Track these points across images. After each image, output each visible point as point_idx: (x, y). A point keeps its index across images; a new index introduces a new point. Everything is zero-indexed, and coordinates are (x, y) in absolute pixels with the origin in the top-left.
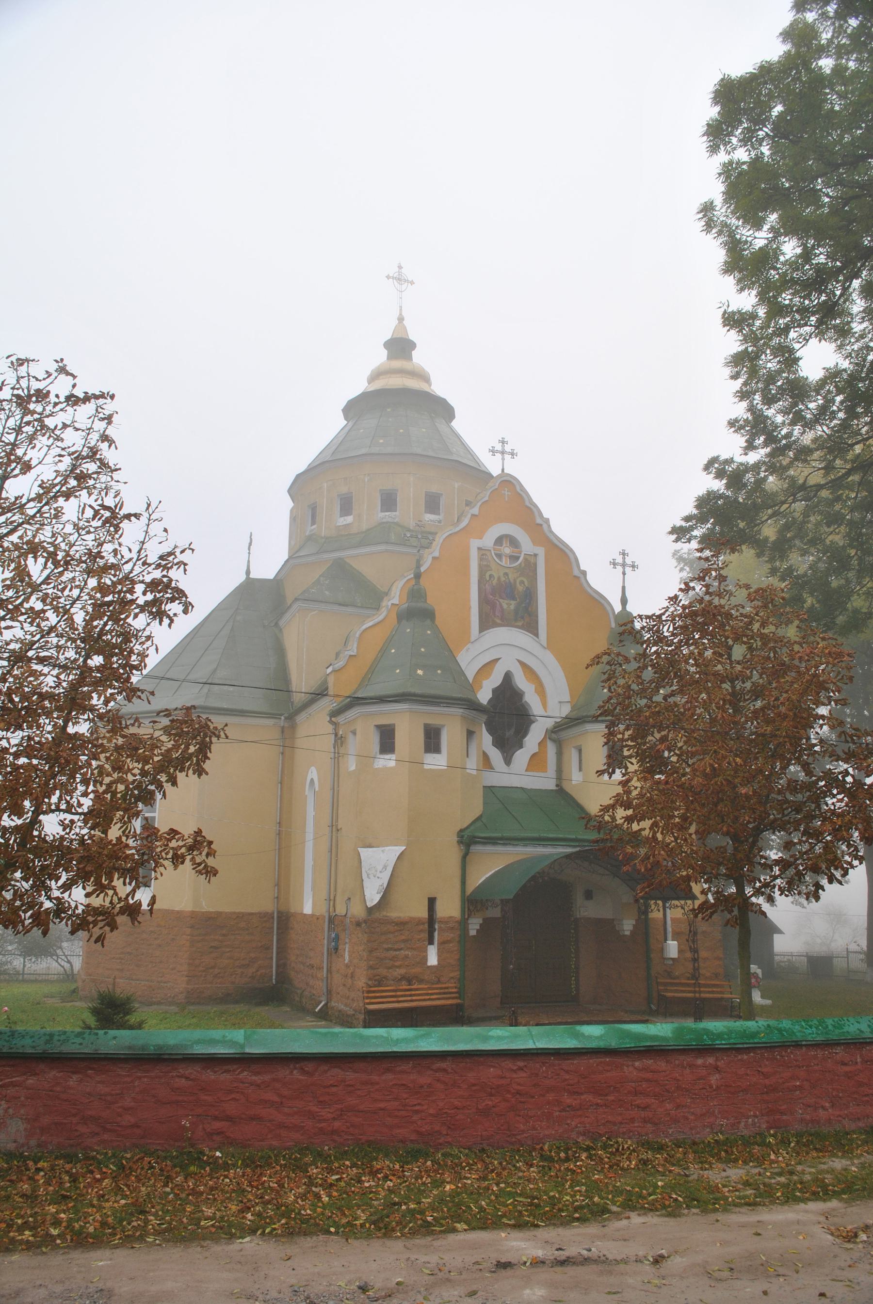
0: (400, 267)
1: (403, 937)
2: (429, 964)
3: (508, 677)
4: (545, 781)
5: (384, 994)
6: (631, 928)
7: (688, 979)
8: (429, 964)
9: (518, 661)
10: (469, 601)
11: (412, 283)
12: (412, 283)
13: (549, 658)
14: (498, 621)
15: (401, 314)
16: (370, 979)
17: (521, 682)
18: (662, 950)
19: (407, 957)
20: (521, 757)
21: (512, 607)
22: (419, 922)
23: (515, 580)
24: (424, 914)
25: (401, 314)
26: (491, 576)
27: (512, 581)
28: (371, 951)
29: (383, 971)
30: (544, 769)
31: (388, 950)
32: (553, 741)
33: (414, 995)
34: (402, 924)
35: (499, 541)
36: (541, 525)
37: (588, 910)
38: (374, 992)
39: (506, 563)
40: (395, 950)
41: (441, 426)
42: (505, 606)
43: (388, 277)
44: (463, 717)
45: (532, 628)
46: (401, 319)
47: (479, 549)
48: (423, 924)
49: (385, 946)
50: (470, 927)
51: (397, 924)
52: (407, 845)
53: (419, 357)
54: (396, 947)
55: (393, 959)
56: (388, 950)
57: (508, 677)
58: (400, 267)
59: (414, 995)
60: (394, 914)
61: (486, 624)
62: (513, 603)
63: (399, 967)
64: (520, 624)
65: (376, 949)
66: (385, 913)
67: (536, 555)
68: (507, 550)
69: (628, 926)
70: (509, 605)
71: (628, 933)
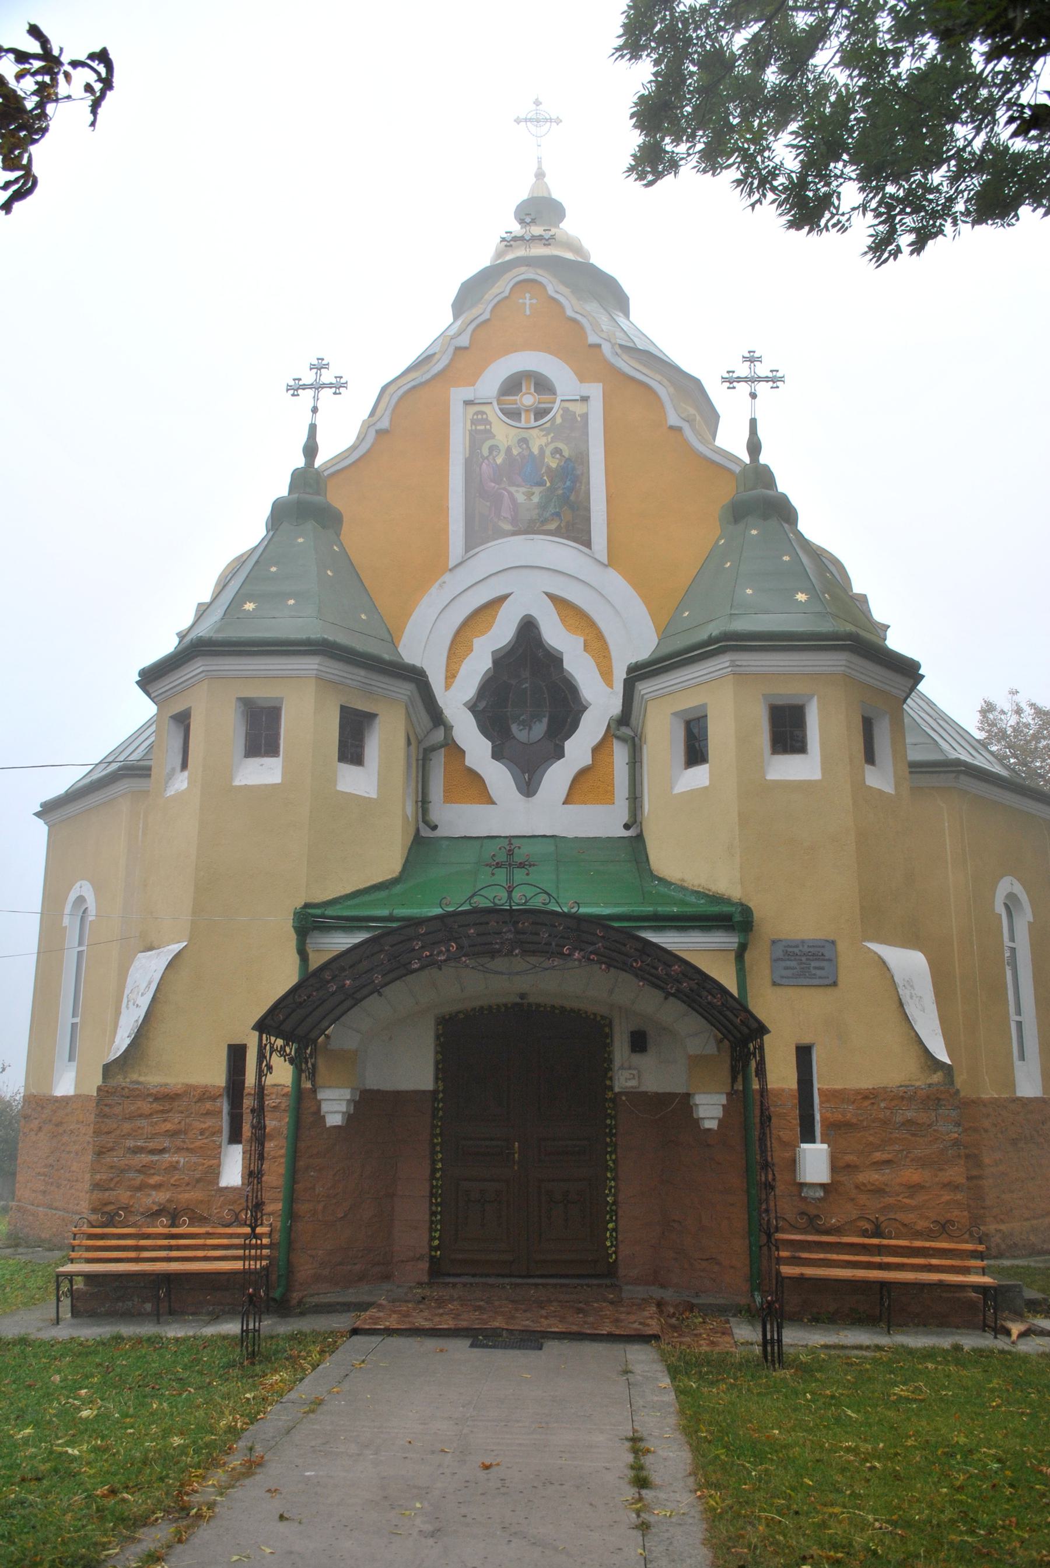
0: (537, 103)
1: (169, 1126)
2: (223, 1183)
3: (528, 628)
4: (604, 821)
5: (225, 1241)
6: (719, 1112)
7: (865, 1234)
8: (223, 1183)
9: (547, 594)
10: (444, 496)
11: (558, 121)
12: (558, 121)
13: (615, 584)
14: (507, 527)
15: (540, 168)
16: (94, 1210)
17: (555, 634)
18: (793, 1164)
19: (174, 1167)
20: (557, 777)
21: (536, 499)
22: (205, 1095)
23: (542, 450)
24: (217, 1077)
25: (540, 168)
26: (492, 449)
27: (536, 451)
28: (100, 1153)
29: (123, 1196)
30: (606, 796)
31: (137, 1151)
32: (623, 739)
33: (178, 1248)
34: (167, 1098)
35: (512, 385)
36: (599, 346)
37: (633, 1075)
38: (103, 1237)
39: (528, 421)
40: (152, 1152)
41: (621, 320)
42: (521, 498)
43: (518, 121)
44: (323, 681)
45: (577, 531)
46: (540, 175)
47: (468, 403)
48: (214, 1098)
49: (130, 1143)
50: (325, 1107)
51: (157, 1099)
52: (189, 941)
53: (569, 226)
54: (151, 1145)
55: (144, 1170)
56: (137, 1151)
57: (528, 628)
58: (537, 103)
59: (178, 1248)
60: (153, 1079)
61: (477, 535)
62: (537, 490)
63: (157, 1187)
64: (553, 526)
65: (112, 1149)
66: (135, 1077)
67: (585, 399)
68: (528, 399)
69: (710, 1109)
70: (524, 497)
71: (712, 1125)
